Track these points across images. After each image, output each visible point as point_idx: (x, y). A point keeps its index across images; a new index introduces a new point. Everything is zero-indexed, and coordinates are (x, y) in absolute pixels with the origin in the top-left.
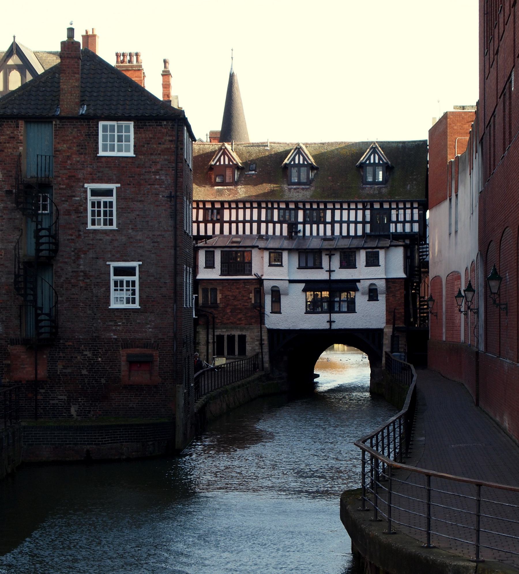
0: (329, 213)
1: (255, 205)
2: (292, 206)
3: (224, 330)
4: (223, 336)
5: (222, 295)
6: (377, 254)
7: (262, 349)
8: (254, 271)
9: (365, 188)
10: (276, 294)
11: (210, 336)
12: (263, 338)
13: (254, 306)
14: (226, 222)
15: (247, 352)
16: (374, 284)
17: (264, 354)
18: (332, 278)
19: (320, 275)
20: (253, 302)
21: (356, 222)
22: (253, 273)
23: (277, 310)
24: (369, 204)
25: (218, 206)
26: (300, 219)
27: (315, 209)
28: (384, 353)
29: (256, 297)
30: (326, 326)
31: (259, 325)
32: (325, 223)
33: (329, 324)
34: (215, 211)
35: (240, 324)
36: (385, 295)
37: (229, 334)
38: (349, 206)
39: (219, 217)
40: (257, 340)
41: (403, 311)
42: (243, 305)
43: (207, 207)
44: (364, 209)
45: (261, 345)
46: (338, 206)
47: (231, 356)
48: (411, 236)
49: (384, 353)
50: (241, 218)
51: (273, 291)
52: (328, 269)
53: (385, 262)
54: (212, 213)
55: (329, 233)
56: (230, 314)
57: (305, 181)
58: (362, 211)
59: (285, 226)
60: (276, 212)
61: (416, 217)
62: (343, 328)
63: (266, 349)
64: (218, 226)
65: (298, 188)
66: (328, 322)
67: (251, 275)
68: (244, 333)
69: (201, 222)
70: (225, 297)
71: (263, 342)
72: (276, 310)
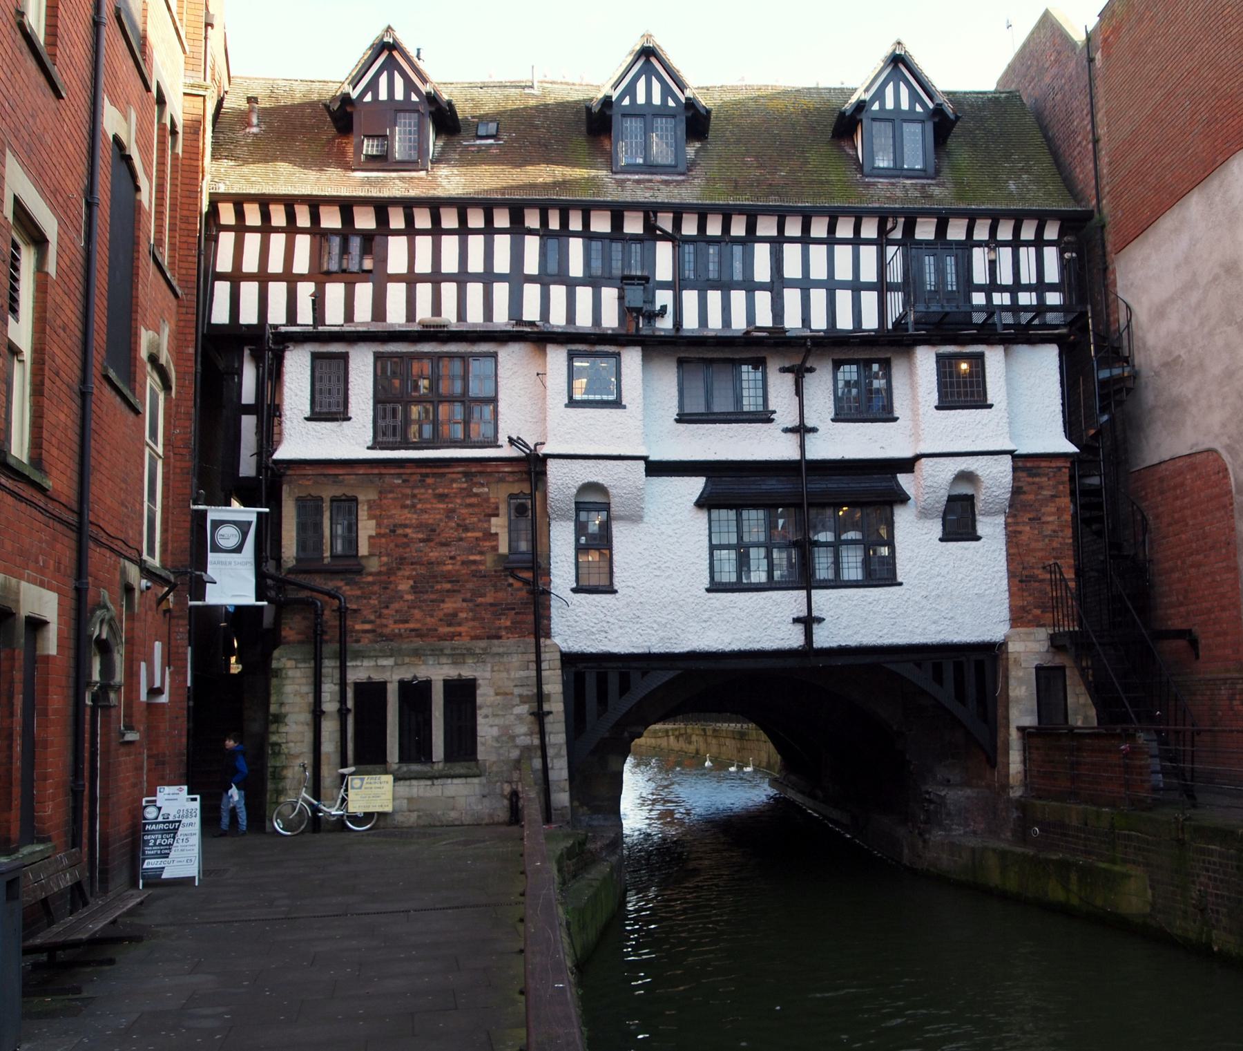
0: (762, 253)
1: (502, 220)
2: (634, 226)
3: (389, 662)
5: (379, 525)
6: (978, 360)
7: (542, 734)
8: (507, 428)
9: (874, 184)
10: (597, 517)
11: (329, 689)
12: (546, 688)
13: (509, 567)
14: (397, 278)
15: (480, 748)
16: (966, 477)
17: (551, 752)
18: (811, 455)
19: (766, 445)
20: (503, 549)
22: (503, 439)
24: (901, 220)
26: (664, 268)
27: (713, 240)
28: (1014, 734)
30: (793, 638)
31: (532, 640)
32: (751, 287)
33: (800, 628)
34: (355, 244)
35: (451, 637)
36: (1001, 519)
37: (408, 676)
38: (832, 229)
39: (368, 264)
40: (523, 699)
42: (463, 563)
43: (325, 224)
44: (882, 242)
45: (540, 716)
46: (793, 228)
47: (415, 767)
49: (1014, 734)
50: (450, 265)
51: (580, 507)
52: (793, 421)
54: (345, 250)
55: (764, 318)
56: (409, 597)
57: (670, 160)
58: (874, 249)
60: (576, 247)
62: (853, 641)
63: (557, 736)
64: (364, 291)
65: (650, 181)
66: (796, 620)
67: (494, 444)
68: (467, 673)
69: (302, 278)
70: (390, 533)
71: (546, 707)
72: (594, 581)
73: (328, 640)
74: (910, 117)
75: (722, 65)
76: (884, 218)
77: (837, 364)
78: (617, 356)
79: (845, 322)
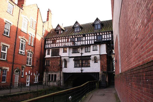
2: (74, 37)
4: (50, 75)
10: (66, 61)
11: (47, 75)
16: (95, 57)
19: (79, 55)
21: (92, 40)
23: (66, 67)
25: (55, 39)
26: (76, 40)
29: (61, 63)
30: (80, 72)
33: (81, 71)
41: (106, 66)
44: (94, 36)
48: (109, 41)
53: (99, 49)
55: (84, 43)
59: (72, 43)
60: (70, 39)
61: (110, 37)
63: (62, 79)
70: (52, 63)
73: (47, 71)
74: (99, 24)
75: (81, 23)
76: (94, 34)
77: (85, 47)
78: (67, 48)
79: (86, 44)
